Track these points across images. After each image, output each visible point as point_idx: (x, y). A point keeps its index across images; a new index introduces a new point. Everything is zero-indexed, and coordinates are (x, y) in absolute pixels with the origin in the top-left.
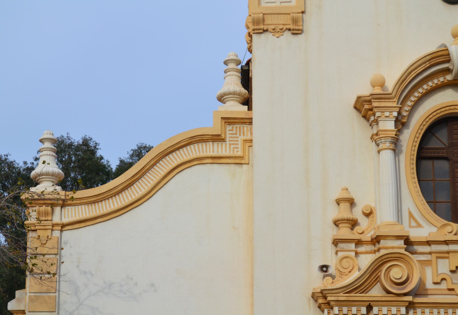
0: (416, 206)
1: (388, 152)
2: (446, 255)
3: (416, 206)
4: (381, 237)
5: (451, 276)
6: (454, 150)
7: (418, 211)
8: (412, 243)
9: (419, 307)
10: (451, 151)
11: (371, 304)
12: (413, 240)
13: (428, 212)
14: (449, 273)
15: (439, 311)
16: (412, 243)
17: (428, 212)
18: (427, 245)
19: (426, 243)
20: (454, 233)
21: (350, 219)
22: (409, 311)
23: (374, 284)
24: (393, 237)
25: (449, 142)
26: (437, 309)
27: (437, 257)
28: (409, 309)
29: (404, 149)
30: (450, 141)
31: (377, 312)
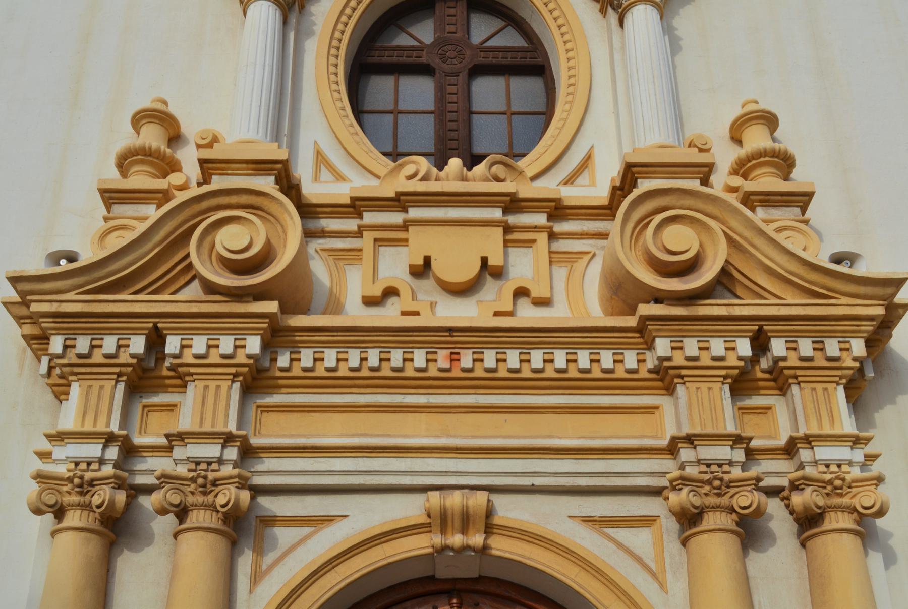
0: (336, 136)
1: (262, 4)
2: (401, 235)
3: (336, 136)
4: (210, 165)
5: (412, 285)
6: (447, 52)
7: (339, 146)
8: (313, 209)
9: (308, 344)
10: (439, 53)
11: (159, 325)
12: (315, 201)
13: (366, 149)
14: (408, 278)
15: (364, 355)
16: (313, 209)
17: (366, 149)
18: (356, 216)
19: (351, 210)
20: (419, 177)
21: (150, 148)
22: (279, 354)
23: (182, 281)
24: (244, 166)
25: (436, 36)
26: (358, 351)
27: (376, 240)
28: (279, 350)
29: (318, 29)
30: (438, 34)
31: (175, 347)
